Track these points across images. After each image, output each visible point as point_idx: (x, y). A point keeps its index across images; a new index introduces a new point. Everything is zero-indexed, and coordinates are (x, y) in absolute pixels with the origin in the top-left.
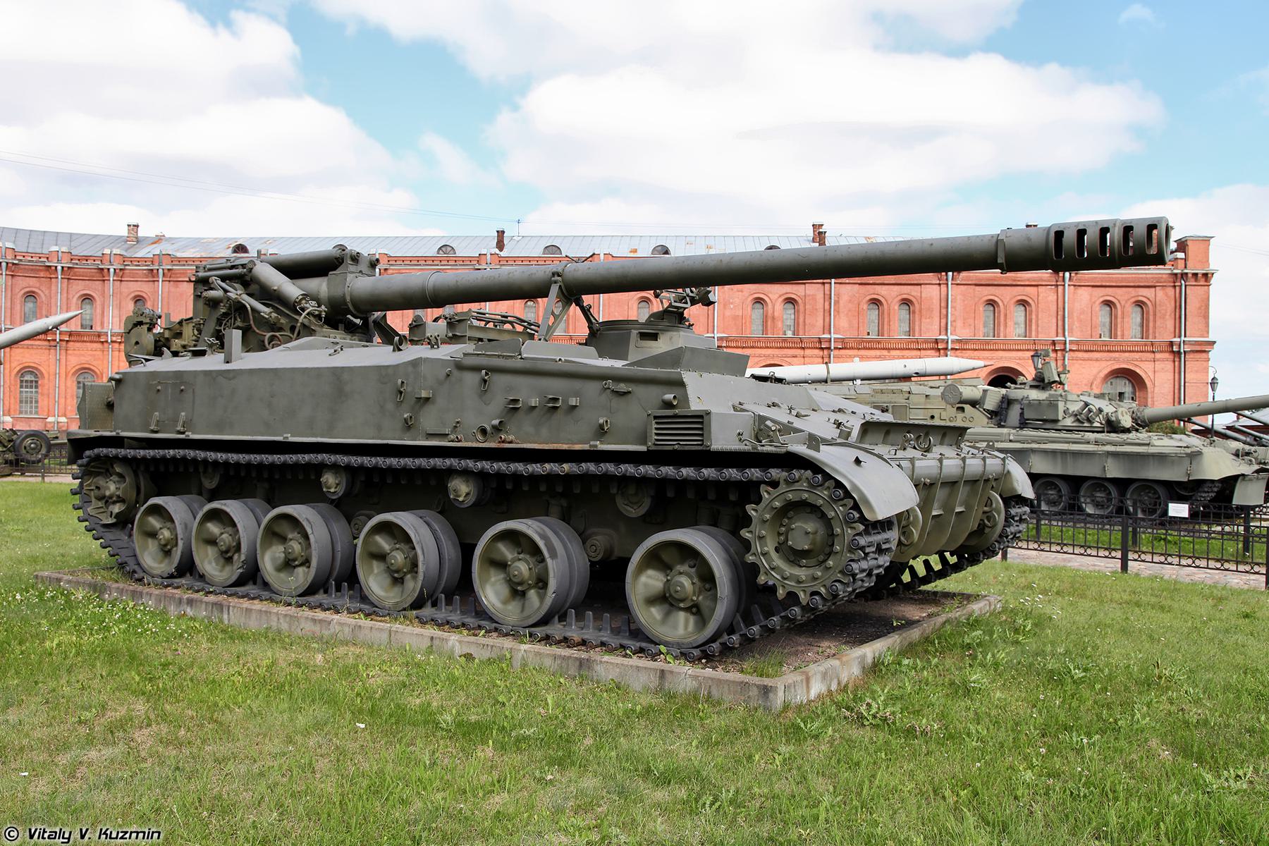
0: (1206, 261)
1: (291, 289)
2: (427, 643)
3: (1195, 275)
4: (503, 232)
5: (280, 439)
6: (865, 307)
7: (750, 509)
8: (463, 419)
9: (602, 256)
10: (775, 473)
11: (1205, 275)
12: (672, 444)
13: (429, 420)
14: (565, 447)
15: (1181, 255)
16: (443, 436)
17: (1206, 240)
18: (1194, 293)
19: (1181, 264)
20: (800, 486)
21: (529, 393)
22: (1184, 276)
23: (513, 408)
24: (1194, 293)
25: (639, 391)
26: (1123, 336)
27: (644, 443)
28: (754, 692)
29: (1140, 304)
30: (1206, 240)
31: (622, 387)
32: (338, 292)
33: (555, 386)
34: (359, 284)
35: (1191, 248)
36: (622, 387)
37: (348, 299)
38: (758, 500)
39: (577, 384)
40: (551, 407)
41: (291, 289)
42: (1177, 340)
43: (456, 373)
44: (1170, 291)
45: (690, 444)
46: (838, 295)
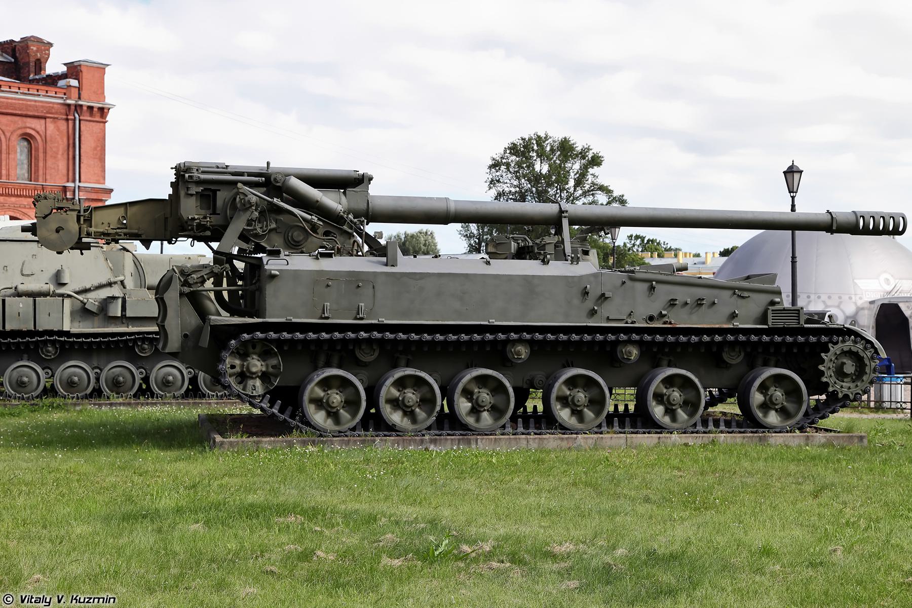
0: (100, 91)
1: (331, 200)
2: (657, 441)
3: (91, 108)
5: (486, 323)
8: (632, 308)
10: (835, 338)
11: (101, 110)
14: (717, 326)
17: (101, 69)
18: (88, 129)
19: (75, 93)
20: (849, 345)
21: (682, 294)
22: (78, 108)
23: (672, 303)
24: (88, 129)
25: (754, 296)
26: (8, 176)
29: (27, 138)
30: (101, 69)
31: (746, 294)
35: (86, 75)
36: (746, 294)
38: (827, 351)
39: (716, 292)
40: (699, 303)
41: (331, 200)
42: (71, 185)
44: (62, 125)
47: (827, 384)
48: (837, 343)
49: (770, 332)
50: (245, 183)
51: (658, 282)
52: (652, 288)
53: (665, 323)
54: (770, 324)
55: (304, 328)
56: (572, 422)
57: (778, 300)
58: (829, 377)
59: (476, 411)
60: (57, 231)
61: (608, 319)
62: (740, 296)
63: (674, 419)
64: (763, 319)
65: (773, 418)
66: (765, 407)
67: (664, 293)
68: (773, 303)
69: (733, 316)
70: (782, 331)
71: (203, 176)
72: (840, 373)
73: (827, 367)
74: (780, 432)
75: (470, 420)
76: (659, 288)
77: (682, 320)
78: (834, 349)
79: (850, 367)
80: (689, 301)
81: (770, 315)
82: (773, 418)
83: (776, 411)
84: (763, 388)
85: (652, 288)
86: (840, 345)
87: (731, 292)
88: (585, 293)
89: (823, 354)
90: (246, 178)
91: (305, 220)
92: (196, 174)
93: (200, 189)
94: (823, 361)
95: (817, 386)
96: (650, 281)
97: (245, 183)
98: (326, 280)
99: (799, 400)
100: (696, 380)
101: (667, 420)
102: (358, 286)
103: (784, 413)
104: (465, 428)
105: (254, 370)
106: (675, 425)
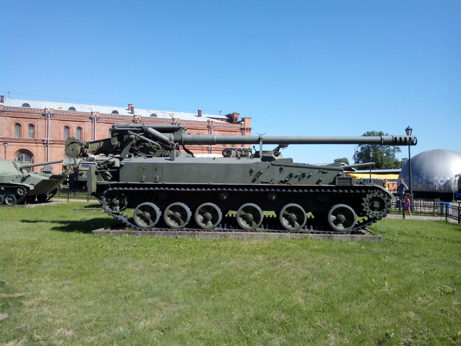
1: (165, 136)
2: (279, 236)
3: (247, 129)
4: (3, 96)
7: (364, 199)
8: (274, 178)
9: (49, 110)
12: (342, 184)
13: (262, 178)
14: (311, 185)
15: (243, 123)
16: (268, 183)
21: (296, 172)
22: (244, 129)
23: (291, 175)
25: (330, 172)
27: (335, 184)
28: (377, 239)
31: (326, 171)
32: (179, 138)
34: (186, 135)
36: (326, 171)
37: (183, 140)
38: (366, 197)
40: (303, 175)
41: (165, 136)
45: (348, 184)
47: (365, 212)
48: (370, 193)
49: (337, 188)
50: (131, 131)
51: (284, 166)
52: (281, 169)
54: (337, 184)
55: (133, 186)
56: (247, 226)
57: (341, 173)
59: (205, 221)
60: (72, 150)
61: (262, 183)
62: (323, 173)
63: (293, 226)
64: (334, 182)
65: (340, 227)
66: (337, 222)
67: (286, 171)
68: (339, 175)
69: (319, 181)
70: (343, 188)
71: (117, 129)
72: (373, 208)
73: (366, 205)
74: (342, 234)
75: (203, 225)
77: (294, 182)
78: (369, 196)
79: (377, 204)
80: (299, 174)
81: (337, 180)
82: (340, 227)
83: (342, 223)
84: (334, 213)
85: (281, 169)
86: (371, 194)
87: (318, 170)
88: (251, 171)
90: (135, 129)
91: (153, 144)
92: (116, 128)
93: (118, 134)
94: (363, 202)
95: (361, 213)
96: (281, 166)
97: (131, 131)
99: (352, 219)
100: (302, 209)
101: (290, 226)
102: (156, 169)
104: (199, 227)
105: (115, 202)
106: (293, 229)
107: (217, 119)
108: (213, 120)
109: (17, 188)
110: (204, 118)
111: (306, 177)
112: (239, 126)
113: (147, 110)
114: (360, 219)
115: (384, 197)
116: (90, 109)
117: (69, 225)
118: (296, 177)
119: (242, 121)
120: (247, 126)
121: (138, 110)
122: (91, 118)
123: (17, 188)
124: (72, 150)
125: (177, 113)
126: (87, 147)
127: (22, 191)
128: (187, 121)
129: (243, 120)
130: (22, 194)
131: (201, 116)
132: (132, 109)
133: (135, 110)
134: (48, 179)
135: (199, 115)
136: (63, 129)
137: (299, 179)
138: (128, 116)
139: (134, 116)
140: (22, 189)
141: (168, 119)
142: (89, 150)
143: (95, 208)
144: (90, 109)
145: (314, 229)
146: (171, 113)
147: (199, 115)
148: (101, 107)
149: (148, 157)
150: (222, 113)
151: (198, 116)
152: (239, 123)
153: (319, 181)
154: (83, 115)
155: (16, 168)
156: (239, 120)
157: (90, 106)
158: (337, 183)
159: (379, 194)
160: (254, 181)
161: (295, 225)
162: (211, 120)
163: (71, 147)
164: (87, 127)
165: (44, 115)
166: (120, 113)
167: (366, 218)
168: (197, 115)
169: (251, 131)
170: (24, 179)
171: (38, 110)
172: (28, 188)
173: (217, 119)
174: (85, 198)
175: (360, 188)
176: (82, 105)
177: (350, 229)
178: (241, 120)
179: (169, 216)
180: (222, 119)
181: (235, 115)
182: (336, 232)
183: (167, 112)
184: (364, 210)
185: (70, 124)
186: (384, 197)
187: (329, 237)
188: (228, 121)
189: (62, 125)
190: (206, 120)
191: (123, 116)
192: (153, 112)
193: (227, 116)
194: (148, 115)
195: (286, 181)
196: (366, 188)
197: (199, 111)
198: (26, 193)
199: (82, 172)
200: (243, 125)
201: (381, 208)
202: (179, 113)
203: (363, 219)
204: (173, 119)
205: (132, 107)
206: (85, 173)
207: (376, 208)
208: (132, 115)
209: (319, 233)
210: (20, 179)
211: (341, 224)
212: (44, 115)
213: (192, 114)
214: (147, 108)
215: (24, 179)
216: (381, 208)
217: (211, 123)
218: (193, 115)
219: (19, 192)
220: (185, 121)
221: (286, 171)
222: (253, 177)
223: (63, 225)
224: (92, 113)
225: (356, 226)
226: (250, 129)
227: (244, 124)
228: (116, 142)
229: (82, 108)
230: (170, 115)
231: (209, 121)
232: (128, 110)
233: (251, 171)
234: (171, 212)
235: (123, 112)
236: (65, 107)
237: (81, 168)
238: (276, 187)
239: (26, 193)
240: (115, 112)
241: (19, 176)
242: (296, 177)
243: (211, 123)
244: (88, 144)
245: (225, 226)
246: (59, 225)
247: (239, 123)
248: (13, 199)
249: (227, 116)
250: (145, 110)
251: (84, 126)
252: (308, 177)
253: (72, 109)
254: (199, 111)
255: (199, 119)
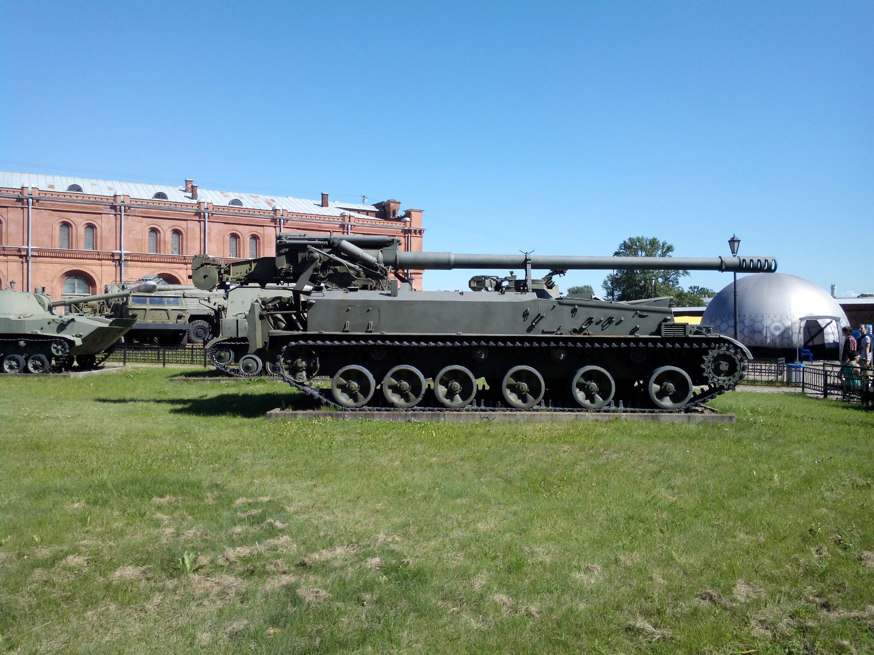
1: (369, 255)
2: (574, 417)
3: (415, 231)
6: (228, 238)
9: (30, 190)
13: (543, 325)
15: (408, 219)
22: (409, 231)
23: (590, 321)
31: (645, 314)
33: (611, 313)
36: (645, 314)
38: (707, 354)
39: (623, 312)
40: (610, 320)
41: (369, 255)
43: (558, 307)
45: (681, 335)
46: (210, 229)
47: (707, 378)
48: (714, 348)
49: (664, 340)
51: (579, 306)
52: (574, 311)
53: (585, 334)
55: (332, 338)
56: (519, 402)
58: (708, 372)
59: (450, 395)
61: (543, 332)
62: (641, 316)
63: (592, 401)
64: (658, 331)
65: (667, 402)
66: (661, 394)
67: (583, 314)
68: (666, 320)
69: (635, 330)
70: (672, 340)
71: (288, 242)
72: (717, 372)
73: (707, 366)
74: (671, 412)
75: (447, 401)
76: (580, 310)
77: (595, 332)
78: (713, 353)
79: (724, 366)
80: (602, 319)
81: (663, 329)
82: (667, 402)
83: (670, 396)
84: (658, 381)
85: (574, 311)
86: (716, 350)
87: (633, 313)
88: (526, 314)
89: (704, 357)
90: (317, 242)
91: (350, 267)
92: (284, 240)
93: (287, 250)
94: (704, 362)
95: (699, 379)
96: (574, 305)
98: (346, 307)
99: (687, 389)
100: (608, 374)
101: (588, 402)
102: (368, 311)
103: (675, 399)
104: (441, 406)
105: (300, 365)
106: (593, 405)
107: (359, 211)
108: (352, 214)
109: (50, 343)
110: (333, 210)
111: (614, 323)
112: (400, 225)
113: (222, 193)
114: (697, 389)
115: (736, 354)
116: (110, 189)
117: (191, 406)
118: (597, 324)
119: (405, 216)
120: (414, 226)
121: (205, 191)
122: (113, 207)
123: (51, 343)
124: (205, 277)
125: (280, 198)
126: (228, 272)
127: (59, 347)
128: (302, 215)
129: (408, 214)
130: (60, 353)
131: (327, 205)
132: (193, 190)
133: (199, 191)
134: (107, 325)
135: (324, 204)
136: (57, 227)
137: (603, 326)
138: (187, 204)
139: (199, 203)
140: (60, 344)
141: (265, 211)
142: (231, 276)
143: (207, 378)
144: (110, 189)
145: (625, 406)
146: (268, 198)
147: (324, 204)
148: (131, 185)
149: (351, 290)
150: (366, 200)
151: (322, 206)
152: (399, 219)
153: (635, 330)
154: (97, 201)
155: (43, 305)
156: (400, 213)
157: (109, 184)
158: (663, 333)
159: (728, 349)
160: (529, 330)
161: (596, 400)
162: (347, 213)
163: (202, 272)
164: (106, 223)
165: (19, 200)
166: (171, 198)
167: (706, 388)
168: (320, 203)
169: (424, 235)
170: (62, 327)
171: (8, 189)
172: (71, 343)
173: (359, 211)
174: (119, 360)
175: (699, 341)
176: (94, 181)
177: (683, 404)
178: (403, 214)
179: (390, 387)
180: (367, 212)
181: (392, 204)
182: (663, 409)
183: (261, 196)
184: (705, 375)
185: (73, 219)
186: (736, 354)
187: (653, 417)
188: (378, 215)
189: (55, 220)
190: (338, 213)
191: (176, 203)
192: (233, 196)
193: (376, 206)
194: (225, 202)
195: (581, 330)
196: (709, 341)
197: (323, 195)
198: (68, 351)
199: (136, 312)
200: (408, 224)
201: (731, 372)
202: (285, 198)
203: (702, 389)
204: (275, 210)
205: (193, 187)
206: (140, 314)
207: (722, 372)
208: (195, 201)
209: (634, 412)
210: (56, 326)
211: (668, 398)
212: (19, 200)
213: (309, 201)
214: (223, 188)
215: (62, 327)
216: (731, 372)
217: (347, 219)
218: (312, 202)
219: (54, 351)
220: (297, 214)
221: (583, 314)
222: (528, 323)
223: (179, 407)
224: (115, 196)
225: (692, 400)
226: (420, 232)
227: (410, 222)
228: (283, 264)
229: (95, 187)
230: (268, 203)
231: (343, 216)
232: (185, 191)
233: (526, 314)
234: (394, 381)
235: (176, 195)
236: (61, 184)
237: (131, 304)
238: (565, 340)
239: (68, 351)
240: (160, 195)
241: (53, 320)
242: (597, 324)
243: (347, 219)
244: (229, 267)
245: (482, 404)
246: (179, 407)
247: (399, 219)
248: (42, 362)
249: (376, 206)
250: (218, 192)
251: (99, 222)
252: (617, 324)
253: (76, 188)
254: (323, 195)
255: (324, 211)
